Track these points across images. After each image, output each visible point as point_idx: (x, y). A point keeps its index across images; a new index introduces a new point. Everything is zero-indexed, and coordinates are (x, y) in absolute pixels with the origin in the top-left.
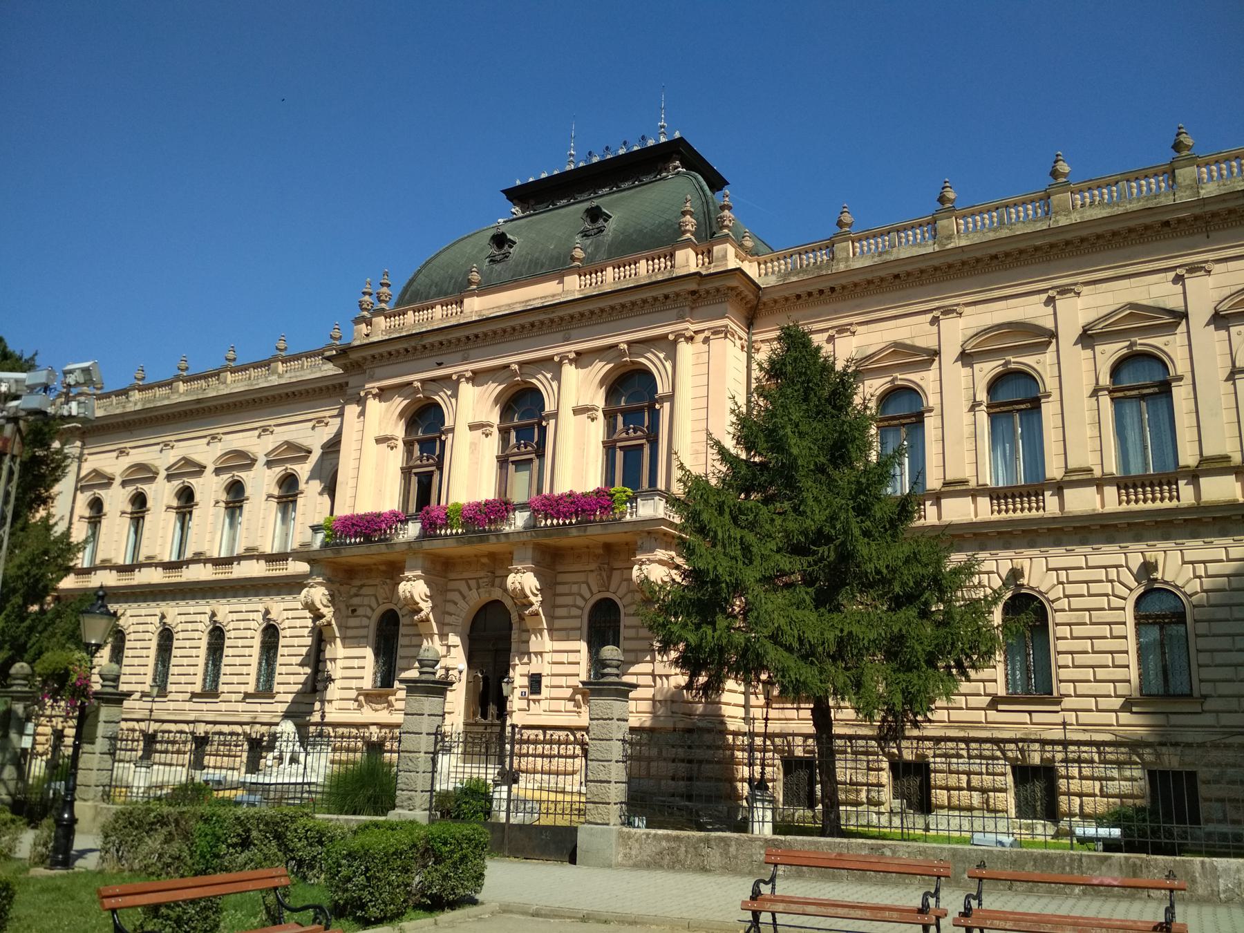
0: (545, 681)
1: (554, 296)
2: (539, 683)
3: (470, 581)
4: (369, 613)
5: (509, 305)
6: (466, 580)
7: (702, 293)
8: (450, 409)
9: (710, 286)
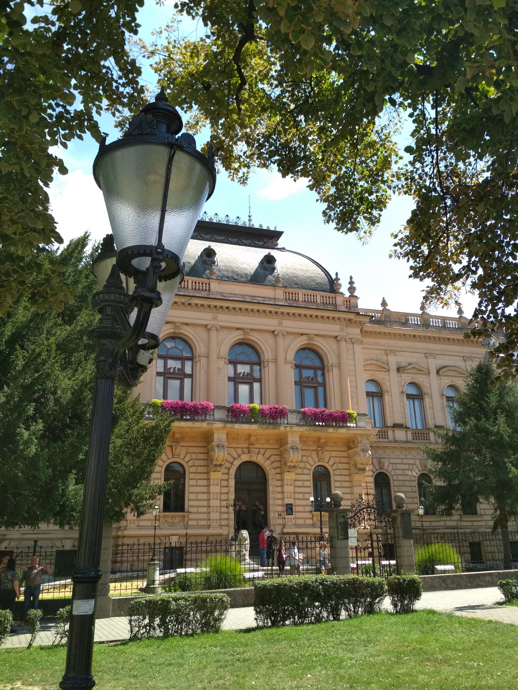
1: (270, 298)
2: (291, 509)
3: (237, 449)
5: (242, 295)
6: (235, 448)
7: (353, 321)
8: (201, 345)
9: (359, 319)
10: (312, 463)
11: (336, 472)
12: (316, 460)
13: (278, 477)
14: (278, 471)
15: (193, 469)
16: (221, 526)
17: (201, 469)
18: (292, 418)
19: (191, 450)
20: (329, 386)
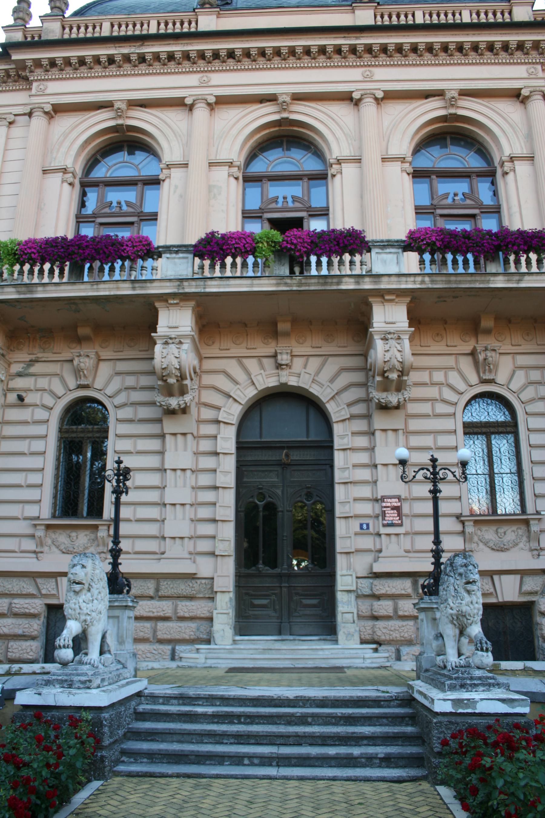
0: (406, 509)
2: (398, 509)
3: (245, 361)
4: (49, 400)
10: (462, 386)
11: (531, 408)
12: (473, 378)
13: (361, 425)
14: (359, 409)
15: (123, 414)
16: (195, 554)
17: (144, 412)
18: (384, 262)
19: (122, 366)
20: (509, 209)
